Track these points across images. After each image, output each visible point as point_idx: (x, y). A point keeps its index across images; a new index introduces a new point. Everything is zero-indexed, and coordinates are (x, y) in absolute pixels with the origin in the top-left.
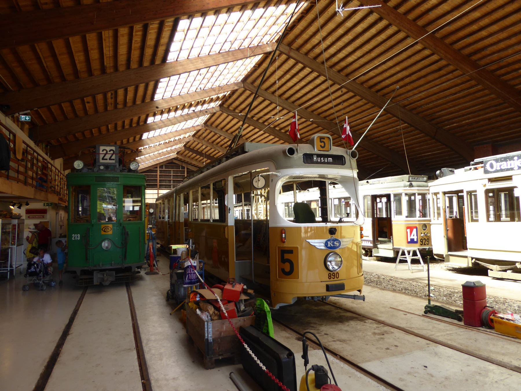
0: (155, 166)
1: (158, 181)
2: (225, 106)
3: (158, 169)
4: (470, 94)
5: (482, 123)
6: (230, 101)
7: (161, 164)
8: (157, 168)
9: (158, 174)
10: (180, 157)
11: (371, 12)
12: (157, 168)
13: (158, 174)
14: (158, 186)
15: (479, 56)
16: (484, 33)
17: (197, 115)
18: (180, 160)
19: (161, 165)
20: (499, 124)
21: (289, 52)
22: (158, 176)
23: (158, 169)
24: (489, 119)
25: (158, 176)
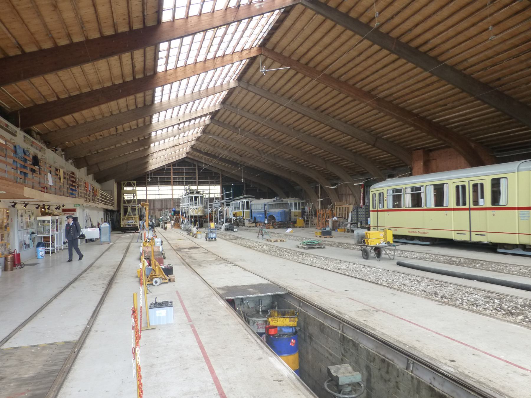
0: (169, 165)
3: (172, 167)
9: (172, 171)
12: (170, 166)
13: (172, 171)
18: (190, 159)
19: (174, 164)
23: (172, 167)
25: (172, 174)
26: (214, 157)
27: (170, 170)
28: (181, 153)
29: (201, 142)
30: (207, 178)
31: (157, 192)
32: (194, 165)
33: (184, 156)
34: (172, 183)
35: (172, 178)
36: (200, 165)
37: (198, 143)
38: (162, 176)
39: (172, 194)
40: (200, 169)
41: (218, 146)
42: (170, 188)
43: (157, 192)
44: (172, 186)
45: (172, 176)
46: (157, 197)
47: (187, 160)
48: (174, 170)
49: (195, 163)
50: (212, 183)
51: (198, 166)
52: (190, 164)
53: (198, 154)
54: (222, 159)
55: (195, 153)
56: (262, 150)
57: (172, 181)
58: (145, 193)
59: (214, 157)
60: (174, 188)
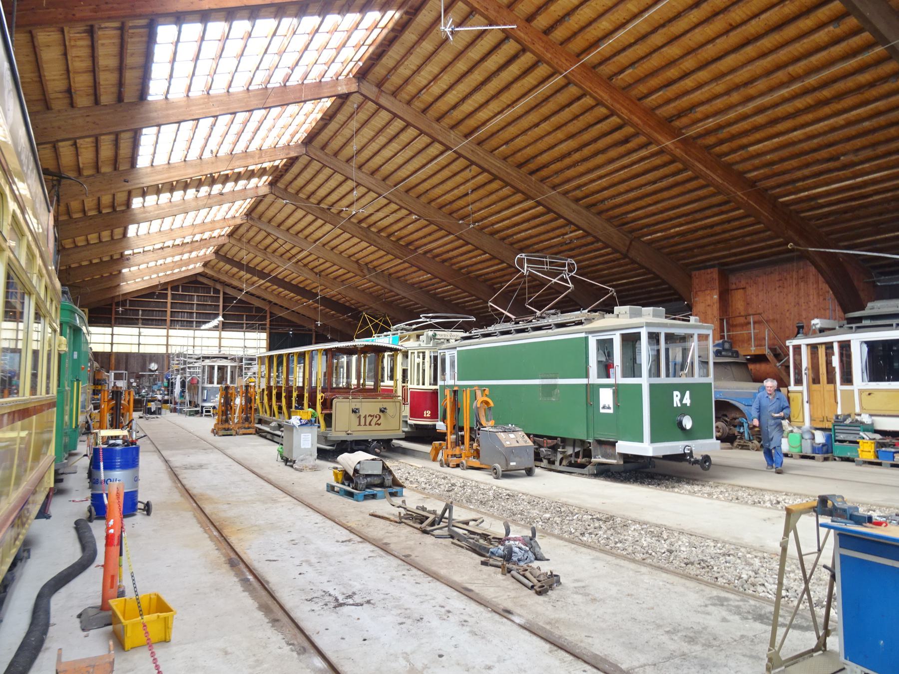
0: (164, 286)
1: (169, 313)
2: (281, 185)
3: (169, 292)
4: (677, 184)
5: (700, 233)
6: (289, 177)
7: (175, 284)
8: (166, 290)
9: (169, 300)
10: (207, 271)
11: (507, 36)
12: (166, 290)
13: (169, 300)
14: (168, 322)
15: (685, 120)
16: (689, 83)
17: (233, 197)
20: (727, 235)
21: (378, 97)
22: (169, 305)
23: (169, 292)
24: (712, 226)
25: (169, 305)
26: (262, 275)
27: (165, 296)
28: (192, 264)
29: (240, 240)
30: (240, 317)
31: (135, 340)
32: (217, 291)
33: (196, 267)
34: (168, 322)
35: (169, 313)
36: (229, 291)
37: (233, 241)
38: (145, 308)
39: (167, 345)
40: (227, 299)
41: (275, 251)
42: (163, 332)
43: (135, 340)
44: (168, 329)
45: (169, 309)
46: (134, 349)
47: (201, 279)
48: (173, 296)
49: (218, 287)
50: (251, 328)
51: (224, 293)
52: (207, 288)
53: (228, 267)
54: (276, 281)
55: (222, 264)
56: (367, 264)
57: (168, 318)
58: (108, 339)
59: (262, 275)
60: (172, 332)
